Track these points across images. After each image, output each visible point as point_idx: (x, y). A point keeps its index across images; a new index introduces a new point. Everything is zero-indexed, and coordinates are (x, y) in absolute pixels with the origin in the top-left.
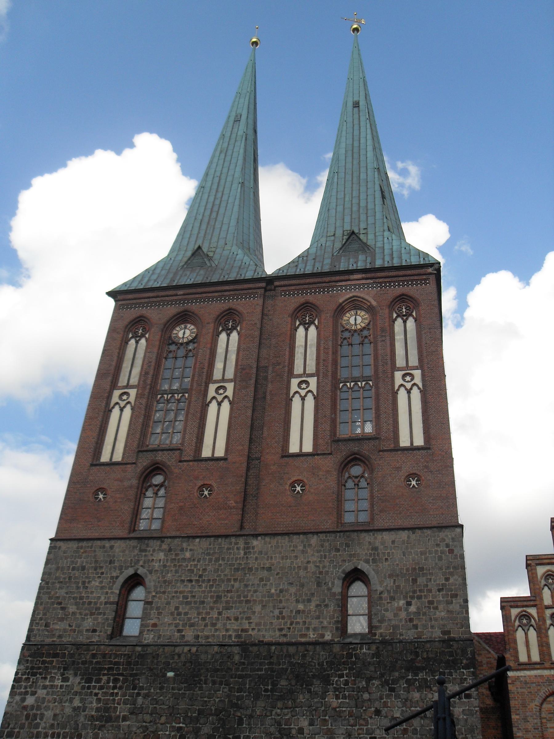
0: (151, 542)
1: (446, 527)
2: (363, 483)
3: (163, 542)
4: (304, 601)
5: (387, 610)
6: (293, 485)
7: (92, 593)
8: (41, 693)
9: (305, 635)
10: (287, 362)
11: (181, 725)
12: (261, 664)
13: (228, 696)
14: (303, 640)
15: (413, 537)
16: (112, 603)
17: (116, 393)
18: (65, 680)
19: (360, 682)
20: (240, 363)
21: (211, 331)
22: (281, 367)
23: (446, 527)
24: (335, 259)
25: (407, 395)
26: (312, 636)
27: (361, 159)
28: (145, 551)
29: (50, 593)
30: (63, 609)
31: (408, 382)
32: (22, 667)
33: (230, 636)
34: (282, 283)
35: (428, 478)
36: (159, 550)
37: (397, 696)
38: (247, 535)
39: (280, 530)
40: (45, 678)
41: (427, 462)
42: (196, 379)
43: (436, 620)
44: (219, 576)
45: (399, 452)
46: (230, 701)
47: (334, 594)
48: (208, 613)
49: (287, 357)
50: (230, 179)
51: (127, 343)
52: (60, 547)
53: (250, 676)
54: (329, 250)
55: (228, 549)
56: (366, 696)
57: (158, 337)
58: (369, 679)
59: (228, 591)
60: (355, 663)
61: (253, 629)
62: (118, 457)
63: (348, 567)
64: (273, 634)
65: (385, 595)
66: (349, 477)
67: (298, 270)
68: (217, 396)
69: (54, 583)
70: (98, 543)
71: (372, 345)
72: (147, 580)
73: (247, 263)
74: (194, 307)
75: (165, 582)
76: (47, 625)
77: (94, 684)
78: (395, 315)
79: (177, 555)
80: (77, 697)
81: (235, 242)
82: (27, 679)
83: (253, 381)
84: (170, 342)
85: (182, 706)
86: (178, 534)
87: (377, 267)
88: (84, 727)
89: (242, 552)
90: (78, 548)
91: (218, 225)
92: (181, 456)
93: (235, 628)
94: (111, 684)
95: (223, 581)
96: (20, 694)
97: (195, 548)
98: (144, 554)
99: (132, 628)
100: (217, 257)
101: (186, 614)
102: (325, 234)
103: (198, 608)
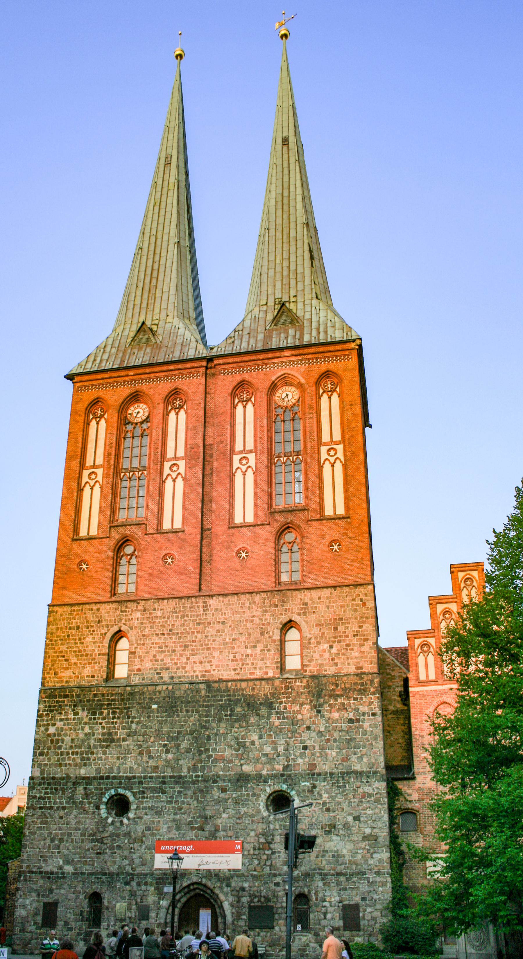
1: (361, 585)
2: (295, 548)
3: (138, 603)
4: (251, 647)
5: (315, 652)
6: (238, 552)
7: (87, 647)
8: (59, 724)
9: (253, 673)
10: (229, 440)
11: (166, 742)
12: (221, 696)
13: (199, 721)
14: (252, 677)
15: (335, 593)
16: (103, 654)
17: (86, 473)
18: (76, 714)
19: (295, 706)
20: (188, 443)
21: (161, 411)
22: (224, 445)
23: (361, 585)
24: (268, 335)
25: (331, 468)
26: (259, 674)
27: (291, 213)
28: (126, 611)
29: (54, 648)
30: (66, 660)
31: (332, 456)
32: (42, 706)
33: (197, 676)
36: (136, 610)
37: (323, 716)
38: (204, 596)
39: (230, 590)
40: (61, 713)
41: (347, 530)
42: (152, 458)
43: (351, 659)
44: (185, 629)
45: (324, 521)
46: (200, 724)
47: (274, 641)
49: (229, 436)
50: (166, 238)
51: (88, 424)
52: (57, 612)
53: (213, 705)
54: (262, 322)
55: (191, 607)
57: (115, 419)
58: (301, 705)
59: (193, 641)
60: (291, 693)
61: (214, 670)
62: (94, 532)
64: (229, 673)
65: (313, 641)
66: (284, 543)
67: (235, 348)
68: (171, 473)
69: (56, 641)
70: (87, 606)
71: (301, 421)
72: (129, 635)
73: (189, 339)
74: (144, 387)
75: (143, 636)
76: (56, 674)
77: (98, 716)
78: (321, 391)
79: (150, 614)
80: (87, 727)
81: (176, 314)
82: (47, 715)
83: (201, 459)
84: (127, 422)
85: (165, 729)
86: (150, 596)
88: (95, 747)
89: (202, 610)
90: (71, 611)
92: (146, 530)
93: (201, 669)
94: (111, 715)
95: (188, 633)
96: (44, 725)
97: (164, 607)
98: (124, 614)
99: (121, 672)
100: (160, 331)
101: (162, 660)
102: (258, 304)
103: (171, 655)
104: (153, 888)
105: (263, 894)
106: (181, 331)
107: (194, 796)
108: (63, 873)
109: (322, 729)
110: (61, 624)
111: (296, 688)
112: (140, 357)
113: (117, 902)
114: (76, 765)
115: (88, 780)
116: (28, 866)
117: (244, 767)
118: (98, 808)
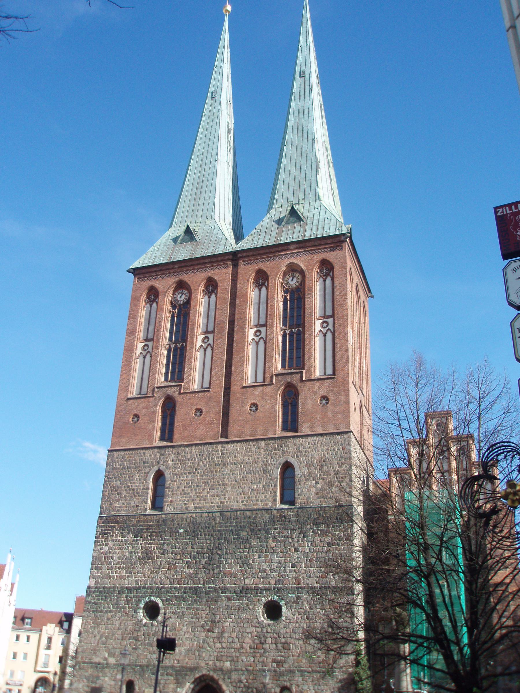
0: (167, 450)
7: (135, 483)
8: (111, 544)
14: (255, 507)
18: (123, 536)
20: (216, 320)
26: (261, 505)
28: (163, 455)
30: (118, 494)
31: (325, 327)
33: (214, 506)
34: (244, 254)
35: (333, 398)
41: (333, 387)
48: (201, 493)
56: (290, 540)
59: (213, 479)
61: (227, 502)
63: (282, 460)
75: (175, 474)
82: (103, 537)
87: (306, 238)
90: (124, 455)
91: (201, 202)
104: (173, 678)
105: (255, 686)
106: (215, 231)
107: (207, 604)
108: (107, 664)
109: (308, 551)
110: (116, 465)
111: (287, 516)
112: (183, 253)
113: (147, 688)
114: (121, 577)
115: (129, 590)
116: (82, 658)
117: (247, 581)
118: (136, 612)
